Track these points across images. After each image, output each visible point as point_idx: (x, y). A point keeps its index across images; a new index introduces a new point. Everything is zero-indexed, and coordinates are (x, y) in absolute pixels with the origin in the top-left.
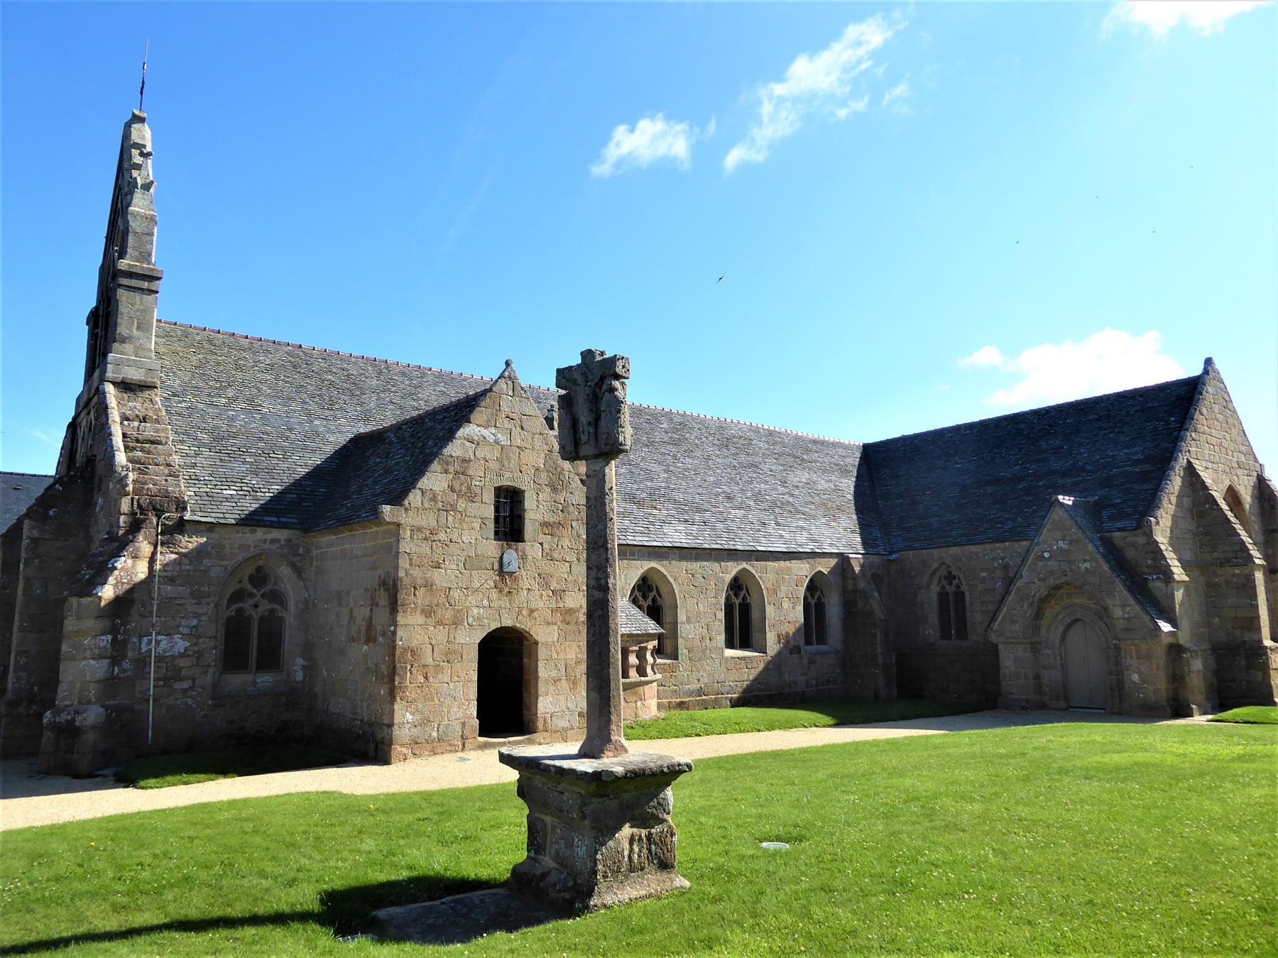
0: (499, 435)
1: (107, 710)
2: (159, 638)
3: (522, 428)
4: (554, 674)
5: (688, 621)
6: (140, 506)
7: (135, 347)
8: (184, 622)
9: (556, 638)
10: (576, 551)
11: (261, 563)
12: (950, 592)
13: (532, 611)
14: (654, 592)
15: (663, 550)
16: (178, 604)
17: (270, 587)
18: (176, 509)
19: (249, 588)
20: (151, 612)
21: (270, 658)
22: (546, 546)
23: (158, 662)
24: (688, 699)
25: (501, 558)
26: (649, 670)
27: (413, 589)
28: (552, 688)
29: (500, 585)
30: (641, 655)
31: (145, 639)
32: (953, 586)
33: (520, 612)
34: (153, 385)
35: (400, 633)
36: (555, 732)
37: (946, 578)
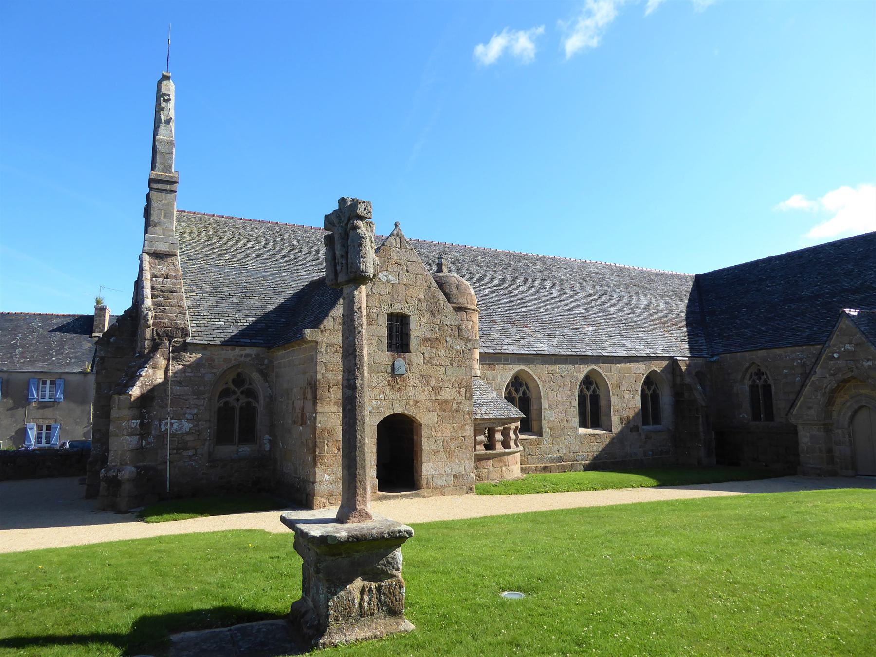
0: (390, 277)
1: (137, 469)
2: (173, 421)
3: (408, 271)
4: (434, 447)
5: (550, 407)
6: (158, 334)
7: (163, 229)
8: (188, 411)
9: (435, 421)
10: (450, 359)
11: (240, 370)
12: (759, 385)
13: (416, 402)
14: (524, 387)
15: (529, 356)
16: (184, 399)
17: (246, 386)
18: (182, 335)
19: (233, 387)
20: (167, 405)
21: (248, 434)
22: (427, 355)
23: (173, 437)
24: (550, 465)
25: (393, 364)
26: (512, 444)
27: (328, 387)
28: (433, 457)
29: (392, 383)
30: (505, 433)
31: (163, 422)
32: (762, 380)
33: (407, 403)
34: (173, 253)
35: (319, 418)
36: (436, 489)
37: (756, 374)
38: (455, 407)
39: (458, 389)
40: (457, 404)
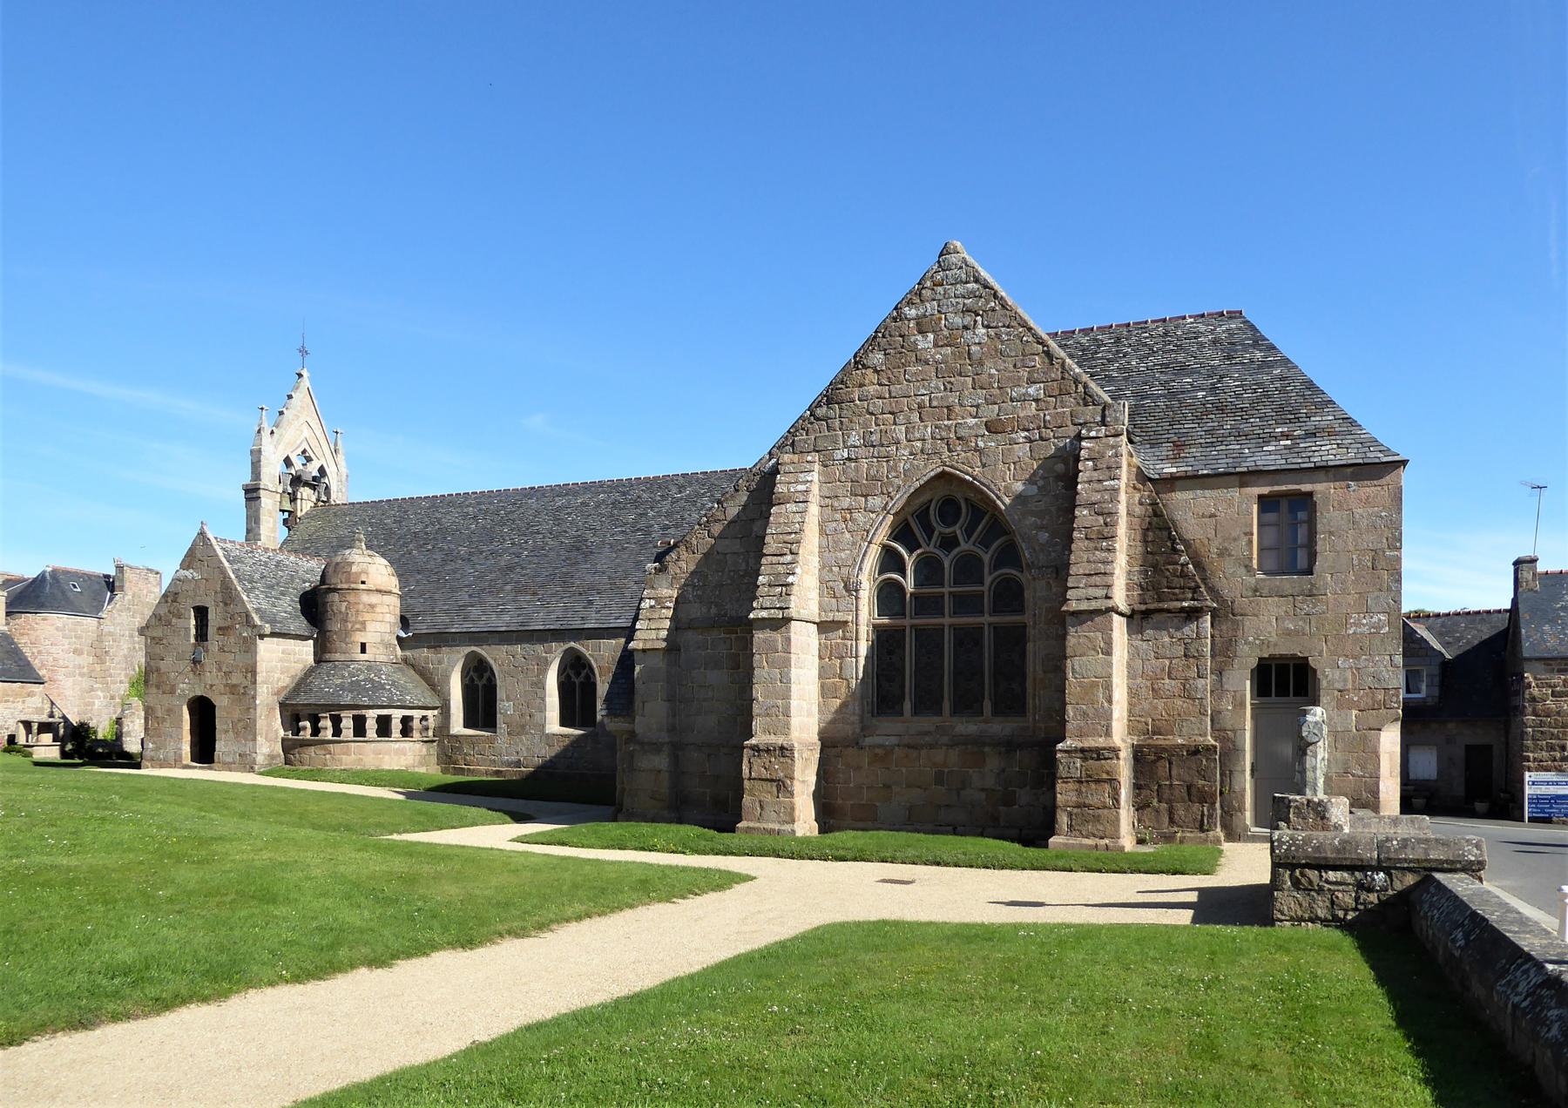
4: (225, 727)
13: (212, 686)
29: (194, 669)
30: (336, 721)
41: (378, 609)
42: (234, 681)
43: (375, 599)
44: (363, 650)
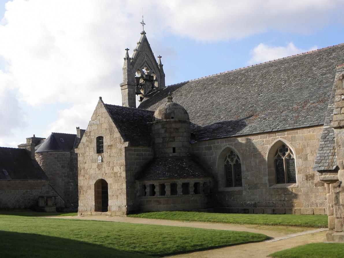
5: (247, 170)
38: (119, 175)
39: (120, 167)
40: (120, 174)
41: (180, 130)
42: (115, 170)
43: (178, 125)
44: (174, 151)
